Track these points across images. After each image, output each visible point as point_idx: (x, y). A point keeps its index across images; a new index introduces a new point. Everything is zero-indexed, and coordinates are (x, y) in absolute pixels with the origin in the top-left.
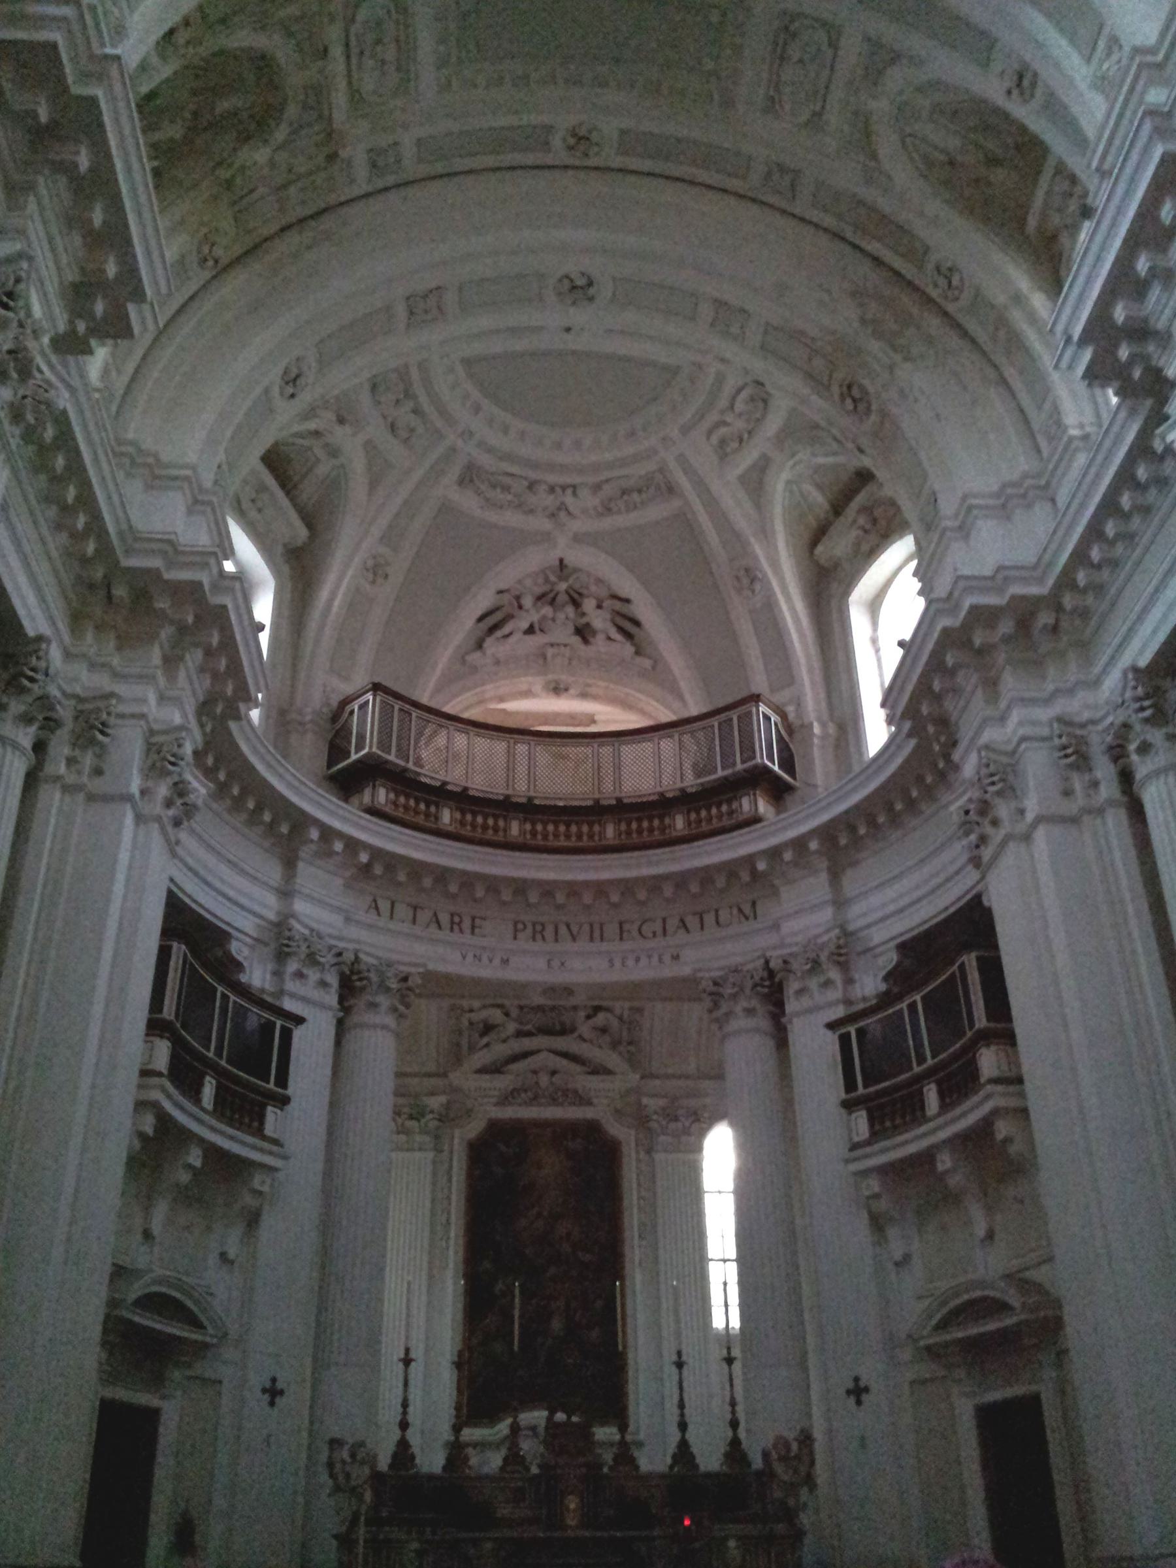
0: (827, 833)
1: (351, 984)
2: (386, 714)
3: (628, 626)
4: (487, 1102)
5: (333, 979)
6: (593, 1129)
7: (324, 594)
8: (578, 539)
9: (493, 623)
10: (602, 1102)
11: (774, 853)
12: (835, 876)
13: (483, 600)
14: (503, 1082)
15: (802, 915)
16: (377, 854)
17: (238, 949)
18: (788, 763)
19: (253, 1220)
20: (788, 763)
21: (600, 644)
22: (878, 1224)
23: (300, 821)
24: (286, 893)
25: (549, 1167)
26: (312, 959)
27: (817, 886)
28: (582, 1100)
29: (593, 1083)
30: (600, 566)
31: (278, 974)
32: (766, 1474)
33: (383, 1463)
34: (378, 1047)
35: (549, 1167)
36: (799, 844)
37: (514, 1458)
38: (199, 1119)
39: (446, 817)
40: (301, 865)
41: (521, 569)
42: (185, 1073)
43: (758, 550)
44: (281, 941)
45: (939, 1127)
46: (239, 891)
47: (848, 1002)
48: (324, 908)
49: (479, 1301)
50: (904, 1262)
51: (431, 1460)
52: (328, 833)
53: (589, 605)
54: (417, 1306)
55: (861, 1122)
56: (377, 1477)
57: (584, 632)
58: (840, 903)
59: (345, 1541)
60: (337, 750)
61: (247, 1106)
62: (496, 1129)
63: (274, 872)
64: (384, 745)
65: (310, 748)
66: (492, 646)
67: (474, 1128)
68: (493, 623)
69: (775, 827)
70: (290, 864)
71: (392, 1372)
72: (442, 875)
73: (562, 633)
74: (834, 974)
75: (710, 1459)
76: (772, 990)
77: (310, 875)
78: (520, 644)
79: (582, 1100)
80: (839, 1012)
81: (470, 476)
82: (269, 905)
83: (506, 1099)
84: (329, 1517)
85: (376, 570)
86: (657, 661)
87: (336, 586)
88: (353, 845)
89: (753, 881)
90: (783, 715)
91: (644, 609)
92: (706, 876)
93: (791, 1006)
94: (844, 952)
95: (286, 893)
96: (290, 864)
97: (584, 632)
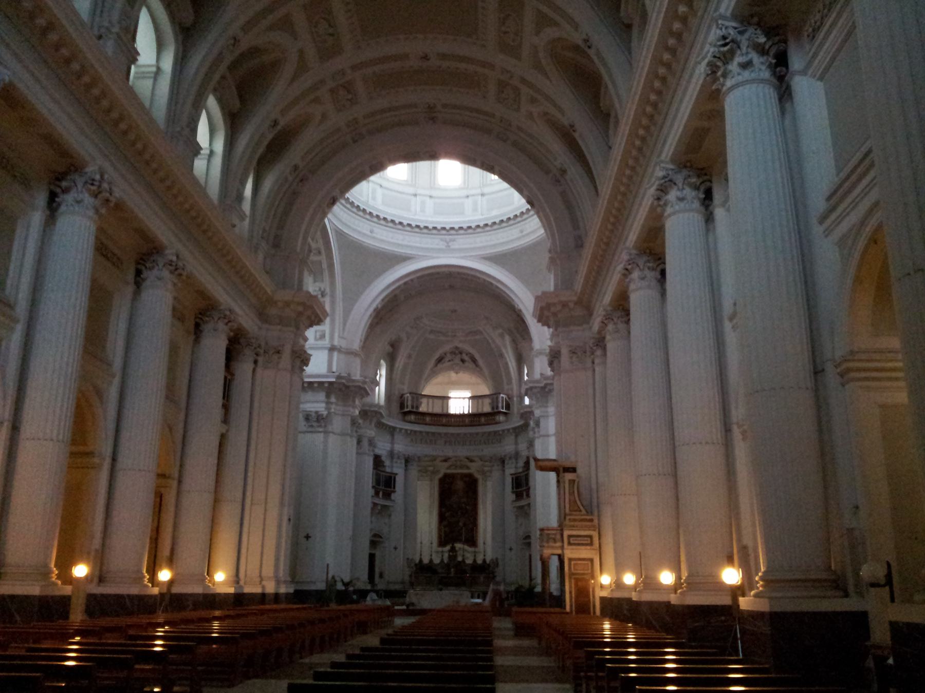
0: (515, 429)
1: (407, 461)
2: (413, 398)
3: (474, 361)
4: (443, 469)
5: (403, 461)
6: (470, 476)
7: (397, 365)
8: (461, 341)
9: (440, 360)
10: (473, 469)
11: (503, 431)
12: (516, 436)
13: (437, 356)
14: (446, 464)
15: (508, 447)
16: (411, 431)
17: (383, 458)
18: (508, 407)
19: (390, 516)
20: (508, 407)
21: (467, 364)
22: (517, 517)
23: (394, 428)
24: (392, 443)
25: (460, 485)
26: (398, 458)
27: (511, 439)
28: (468, 468)
29: (469, 464)
30: (467, 347)
31: (392, 462)
32: (489, 565)
33: (417, 561)
34: (414, 471)
35: (460, 485)
36: (508, 430)
37: (442, 561)
38: (381, 501)
39: (428, 419)
40: (396, 437)
41: (447, 348)
42: (377, 493)
43: (504, 351)
44: (391, 454)
45: (523, 503)
46: (383, 447)
47: (516, 468)
48: (401, 446)
49: (442, 517)
50: (521, 525)
51: (426, 561)
52: (401, 429)
53: (464, 355)
54: (427, 522)
55: (513, 497)
56: (416, 565)
57: (463, 361)
58: (516, 444)
59: (411, 576)
60: (402, 406)
61: (387, 496)
62: (446, 476)
63: (388, 437)
64: (413, 407)
65: (395, 407)
66: (440, 366)
67: (441, 475)
68: (440, 360)
69: (504, 424)
70: (393, 435)
71: (419, 545)
72: (427, 433)
73: (457, 360)
74: (514, 461)
75: (479, 561)
76: (503, 461)
77: (398, 437)
78: (447, 364)
79: (468, 468)
80: (513, 471)
81: (432, 332)
82: (388, 446)
83: (448, 468)
84: (407, 572)
85: (409, 356)
86: (481, 369)
87: (400, 363)
88: (406, 430)
89: (498, 437)
90: (508, 395)
91: (477, 356)
92: (490, 433)
93: (506, 466)
94: (517, 455)
95: (392, 443)
96: (393, 435)
97: (463, 361)
